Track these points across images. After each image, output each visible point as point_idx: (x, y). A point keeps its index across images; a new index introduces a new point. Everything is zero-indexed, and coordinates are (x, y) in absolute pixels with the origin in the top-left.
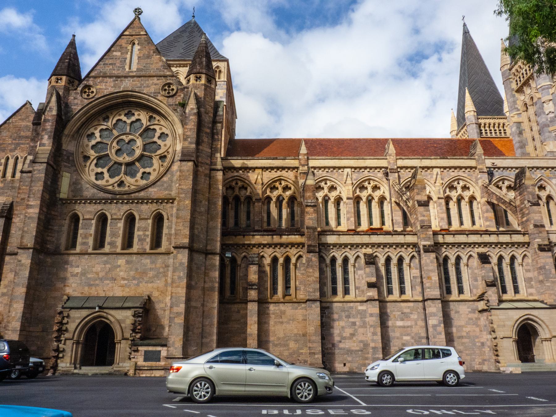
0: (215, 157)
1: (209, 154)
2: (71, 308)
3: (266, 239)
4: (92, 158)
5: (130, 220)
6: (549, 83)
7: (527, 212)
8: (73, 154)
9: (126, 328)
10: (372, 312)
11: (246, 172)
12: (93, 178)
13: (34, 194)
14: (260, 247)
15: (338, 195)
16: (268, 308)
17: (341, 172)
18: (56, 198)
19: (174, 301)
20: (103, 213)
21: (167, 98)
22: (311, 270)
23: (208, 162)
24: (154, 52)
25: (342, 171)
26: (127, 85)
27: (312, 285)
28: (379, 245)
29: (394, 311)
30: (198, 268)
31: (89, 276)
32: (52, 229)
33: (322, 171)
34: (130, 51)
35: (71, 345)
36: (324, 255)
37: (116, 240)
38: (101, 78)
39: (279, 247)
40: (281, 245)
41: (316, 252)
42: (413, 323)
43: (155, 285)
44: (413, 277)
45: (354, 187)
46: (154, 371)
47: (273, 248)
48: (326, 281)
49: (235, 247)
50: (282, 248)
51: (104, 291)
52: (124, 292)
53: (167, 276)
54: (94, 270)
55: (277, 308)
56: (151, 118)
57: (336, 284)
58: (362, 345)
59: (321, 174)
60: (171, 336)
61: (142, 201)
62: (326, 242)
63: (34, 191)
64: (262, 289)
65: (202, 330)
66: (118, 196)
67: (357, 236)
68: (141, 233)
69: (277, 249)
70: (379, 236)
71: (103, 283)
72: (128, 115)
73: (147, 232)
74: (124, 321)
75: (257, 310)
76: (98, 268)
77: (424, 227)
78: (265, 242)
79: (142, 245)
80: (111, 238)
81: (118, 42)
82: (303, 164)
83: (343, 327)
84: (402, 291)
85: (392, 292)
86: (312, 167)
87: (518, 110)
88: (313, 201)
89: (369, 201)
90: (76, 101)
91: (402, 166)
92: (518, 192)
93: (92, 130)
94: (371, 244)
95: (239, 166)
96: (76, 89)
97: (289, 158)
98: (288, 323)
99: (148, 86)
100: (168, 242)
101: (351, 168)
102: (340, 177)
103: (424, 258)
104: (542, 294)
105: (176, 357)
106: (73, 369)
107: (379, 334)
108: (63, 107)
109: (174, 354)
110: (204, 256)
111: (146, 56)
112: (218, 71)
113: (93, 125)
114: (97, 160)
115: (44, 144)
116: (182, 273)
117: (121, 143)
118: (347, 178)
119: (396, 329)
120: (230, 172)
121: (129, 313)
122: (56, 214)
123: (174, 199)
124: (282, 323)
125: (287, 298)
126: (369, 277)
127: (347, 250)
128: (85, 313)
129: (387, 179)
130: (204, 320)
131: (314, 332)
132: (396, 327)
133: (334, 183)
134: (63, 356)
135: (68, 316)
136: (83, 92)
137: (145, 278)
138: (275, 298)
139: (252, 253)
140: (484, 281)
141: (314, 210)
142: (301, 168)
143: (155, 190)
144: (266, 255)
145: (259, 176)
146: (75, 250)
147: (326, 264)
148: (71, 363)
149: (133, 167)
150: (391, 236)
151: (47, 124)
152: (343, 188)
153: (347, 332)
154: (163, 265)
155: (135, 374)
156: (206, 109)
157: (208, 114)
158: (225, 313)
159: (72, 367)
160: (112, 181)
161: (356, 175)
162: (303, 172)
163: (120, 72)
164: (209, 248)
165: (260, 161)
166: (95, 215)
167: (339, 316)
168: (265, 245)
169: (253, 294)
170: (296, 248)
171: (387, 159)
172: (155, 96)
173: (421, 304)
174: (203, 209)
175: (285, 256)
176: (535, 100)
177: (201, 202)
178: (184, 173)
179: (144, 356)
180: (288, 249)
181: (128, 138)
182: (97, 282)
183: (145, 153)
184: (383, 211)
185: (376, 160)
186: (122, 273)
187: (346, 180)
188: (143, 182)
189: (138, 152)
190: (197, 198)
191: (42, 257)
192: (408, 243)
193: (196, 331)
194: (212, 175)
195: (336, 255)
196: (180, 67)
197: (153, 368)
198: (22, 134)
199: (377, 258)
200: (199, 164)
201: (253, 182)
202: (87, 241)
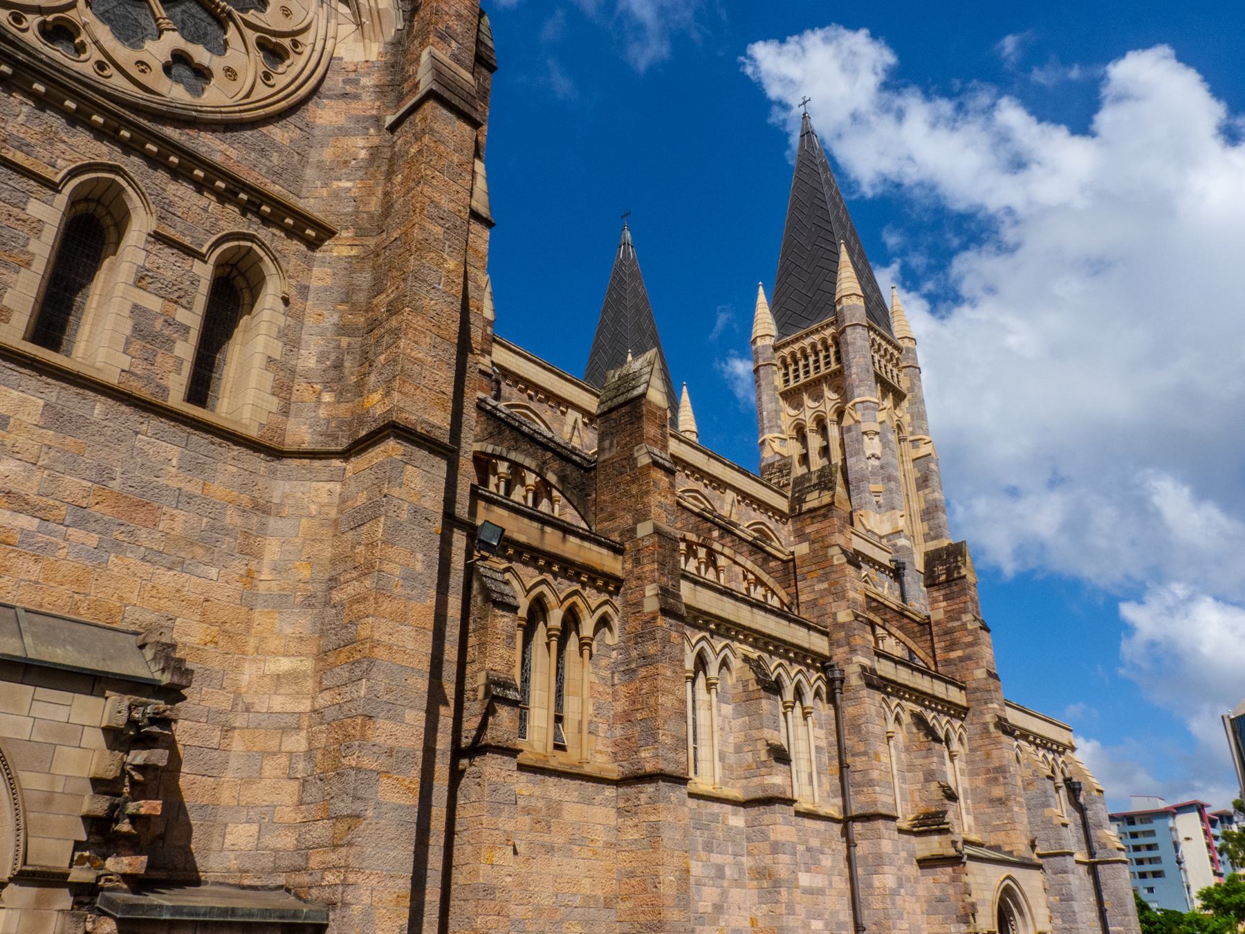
6: (876, 401)
7: (970, 639)
9: (49, 800)
19: (381, 688)
22: (669, 674)
43: (192, 585)
53: (258, 556)
55: (537, 791)
60: (360, 878)
73: (181, 311)
77: (860, 619)
78: (522, 538)
87: (782, 432)
92: (943, 592)
100: (275, 400)
103: (867, 700)
104: (996, 829)
123: (325, 233)
124: (550, 849)
137: (143, 534)
140: (934, 786)
150: (786, 623)
154: (245, 499)
173: (837, 828)
176: (847, 422)
178: (442, 148)
188: (175, 93)
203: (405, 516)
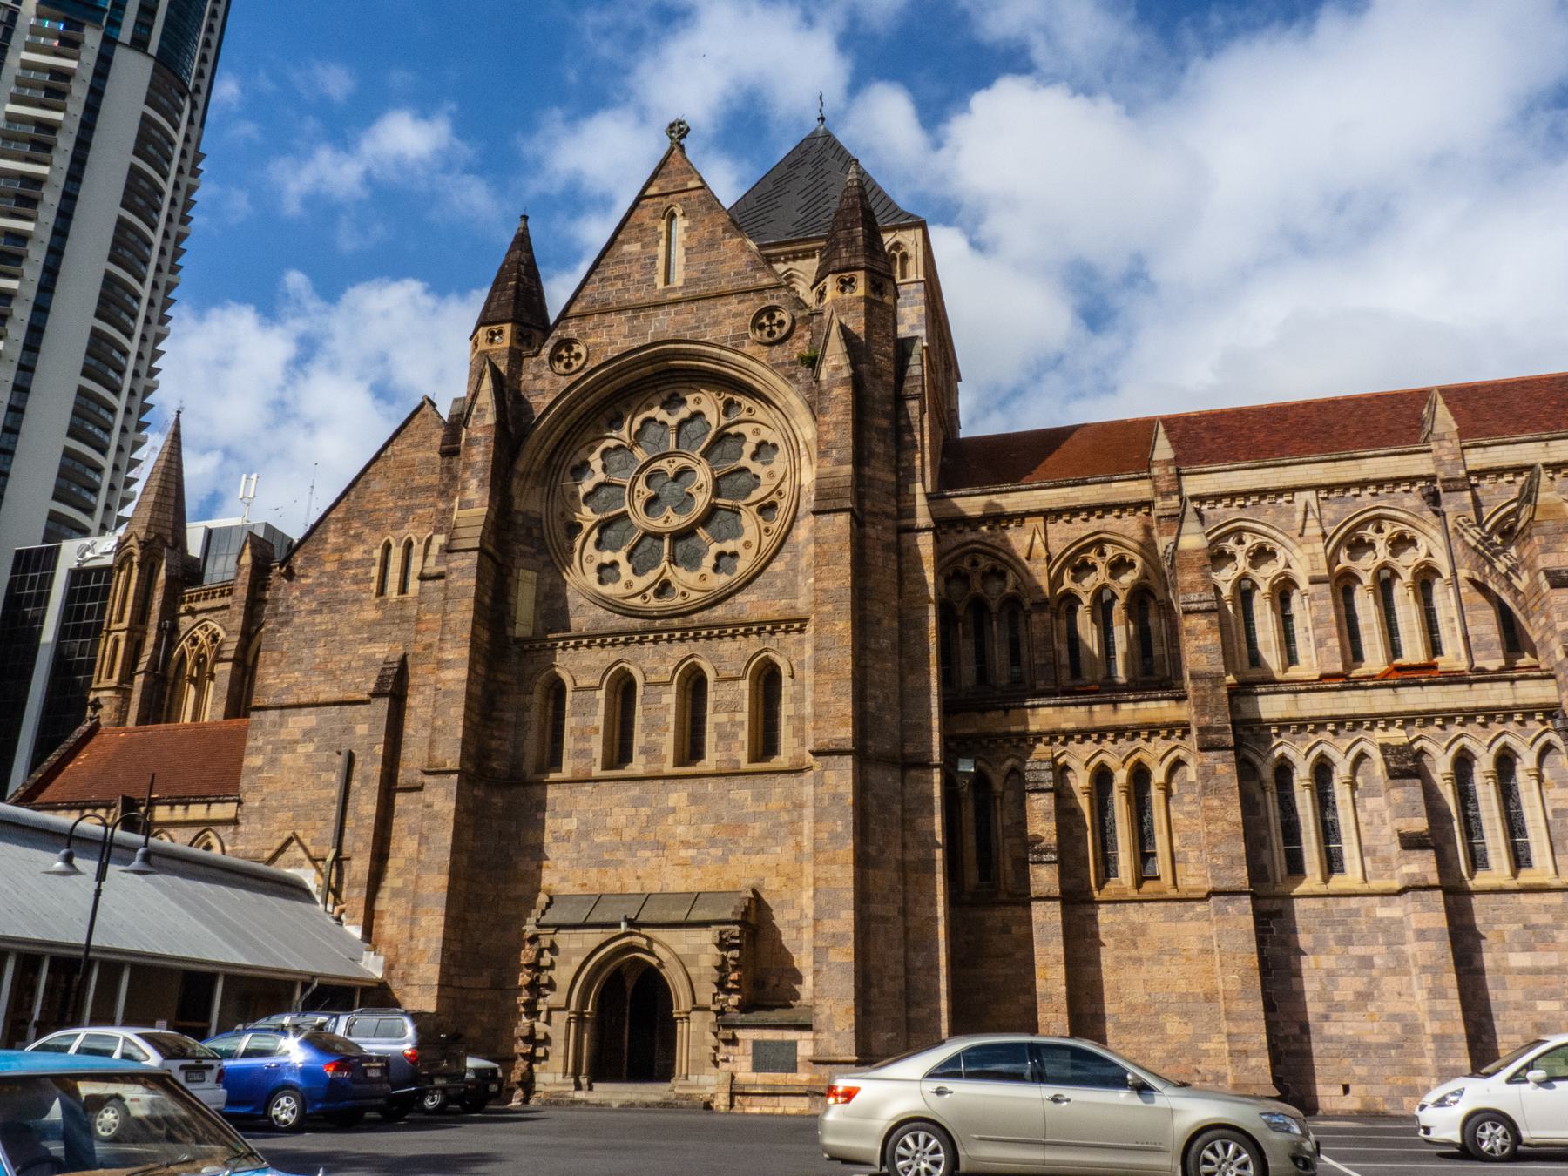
0: (908, 494)
1: (893, 488)
2: (559, 927)
3: (1072, 717)
4: (587, 526)
5: (694, 686)
8: (540, 521)
9: (700, 977)
10: (1424, 926)
12: (592, 577)
13: (453, 632)
14: (1056, 739)
16: (1094, 917)
17: (1285, 505)
18: (507, 638)
19: (823, 902)
21: (767, 349)
22: (1216, 803)
23: (892, 509)
24: (725, 231)
25: (1289, 502)
26: (662, 325)
27: (1223, 848)
28: (1428, 717)
29: (1499, 921)
31: (599, 839)
32: (501, 720)
33: (1226, 506)
34: (664, 235)
35: (563, 1025)
36: (1252, 756)
37: (661, 739)
38: (596, 317)
39: (1111, 736)
40: (1119, 731)
41: (1227, 748)
43: (769, 859)
44: (1555, 811)
46: (781, 1098)
47: (1095, 742)
48: (1264, 833)
49: (985, 742)
50: (1121, 741)
51: (638, 878)
53: (800, 833)
54: (610, 821)
55: (1119, 918)
56: (729, 405)
57: (1299, 842)
58: (1398, 1029)
60: (823, 1002)
61: (721, 630)
62: (1255, 716)
63: (452, 624)
65: (907, 982)
66: (658, 623)
68: (723, 718)
69: (1106, 744)
70: (1426, 689)
71: (635, 856)
74: (694, 959)
76: (619, 817)
78: (1070, 726)
79: (728, 749)
80: (648, 735)
81: (632, 218)
82: (1165, 489)
83: (1331, 974)
84: (1519, 858)
85: (1485, 860)
86: (1193, 498)
88: (1205, 597)
89: (1384, 586)
90: (539, 384)
91: (1485, 466)
93: (582, 454)
94: (1401, 714)
95: (978, 513)
96: (537, 354)
97: (1121, 477)
98: (1158, 962)
99: (716, 323)
100: (796, 740)
101: (1317, 488)
102: (1283, 520)
105: (840, 1059)
106: (573, 1088)
107: (1454, 993)
108: (509, 403)
109: (833, 1050)
110: (897, 773)
112: (898, 255)
114: (601, 532)
115: (469, 501)
116: (839, 823)
117: (659, 481)
119: (1509, 979)
120: (952, 532)
121: (707, 937)
122: (509, 678)
123: (804, 621)
124: (1138, 961)
125: (1148, 887)
126: (1403, 816)
127: (1325, 735)
128: (593, 938)
129: (1436, 513)
130: (912, 954)
131: (1239, 987)
132: (1509, 971)
133: (1266, 539)
135: (553, 949)
136: (555, 357)
137: (741, 841)
138: (1111, 887)
141: (1212, 623)
142: (1159, 503)
143: (753, 597)
144: (1073, 763)
145: (1037, 535)
146: (560, 771)
148: (565, 1073)
149: (692, 542)
150: (1465, 687)
151: (474, 451)
152: (1298, 553)
153: (1347, 989)
154: (789, 804)
155: (732, 1106)
156: (875, 365)
159: (568, 1084)
160: (640, 583)
161: (1335, 507)
162: (1167, 513)
163: (643, 296)
164: (909, 749)
165: (1036, 493)
166: (603, 678)
167: (1316, 939)
168: (1069, 735)
169: (1044, 878)
170: (1165, 738)
171: (1430, 451)
172: (736, 345)
174: (885, 643)
175: (1130, 762)
177: (879, 622)
178: (825, 547)
179: (754, 1054)
180: (1139, 742)
181: (674, 465)
182: (619, 855)
183: (719, 501)
184: (1433, 610)
185: (1396, 458)
186: (680, 830)
187: (1303, 527)
188: (720, 581)
189: (701, 501)
192: (1526, 706)
194: (905, 545)
195: (1291, 754)
196: (795, 259)
197: (777, 1091)
198: (419, 481)
200: (867, 518)
201: (1022, 554)
202: (586, 746)
203: (827, 802)
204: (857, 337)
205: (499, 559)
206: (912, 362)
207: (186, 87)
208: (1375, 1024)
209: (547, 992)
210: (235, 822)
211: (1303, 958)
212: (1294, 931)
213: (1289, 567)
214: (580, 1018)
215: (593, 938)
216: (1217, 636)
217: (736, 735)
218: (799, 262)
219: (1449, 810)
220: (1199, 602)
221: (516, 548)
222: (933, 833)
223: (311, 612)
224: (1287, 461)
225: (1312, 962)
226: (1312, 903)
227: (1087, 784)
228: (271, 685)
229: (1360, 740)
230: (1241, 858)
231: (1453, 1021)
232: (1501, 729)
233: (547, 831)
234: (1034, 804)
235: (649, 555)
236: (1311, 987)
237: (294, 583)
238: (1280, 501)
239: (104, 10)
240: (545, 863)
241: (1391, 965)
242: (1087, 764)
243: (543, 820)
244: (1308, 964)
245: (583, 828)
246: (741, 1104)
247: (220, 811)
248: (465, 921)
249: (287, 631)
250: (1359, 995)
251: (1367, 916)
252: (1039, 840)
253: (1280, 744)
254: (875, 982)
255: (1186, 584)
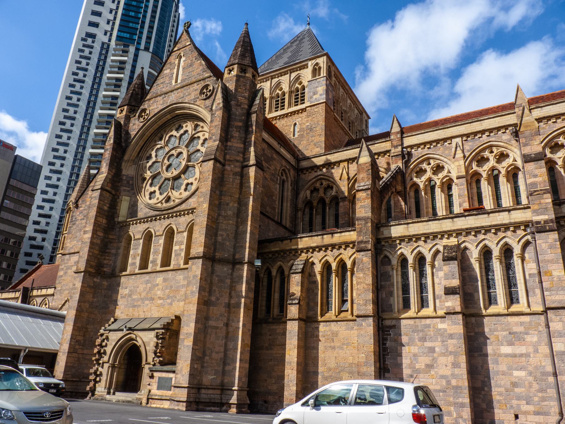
0: (248, 152)
1: (242, 150)
2: (110, 331)
3: (315, 241)
4: (148, 178)
5: (170, 234)
8: (133, 178)
10: (452, 332)
11: (330, 168)
14: (309, 252)
15: (446, 176)
16: (318, 328)
17: (448, 145)
18: (115, 222)
20: (149, 231)
21: (204, 101)
22: (361, 275)
23: (241, 159)
24: (196, 59)
25: (449, 144)
26: (172, 98)
27: (363, 295)
28: (468, 232)
29: (496, 330)
30: (221, 281)
31: (134, 297)
32: (110, 253)
34: (177, 65)
36: (388, 254)
38: (153, 99)
39: (330, 248)
40: (333, 246)
41: (368, 250)
42: (531, 349)
44: (530, 275)
45: (468, 161)
47: (324, 251)
48: (392, 289)
49: (282, 254)
50: (335, 250)
51: (144, 312)
52: (159, 313)
55: (328, 328)
56: (196, 126)
57: (409, 294)
58: (444, 383)
59: (421, 153)
61: (180, 214)
62: (389, 236)
64: (312, 304)
67: (434, 222)
69: (329, 252)
70: (467, 218)
71: (144, 303)
72: (177, 130)
74: (149, 343)
75: (297, 331)
79: (178, 260)
83: (415, 355)
84: (512, 299)
85: (496, 300)
86: (407, 147)
88: (367, 183)
89: (494, 179)
91: (541, 116)
93: (149, 152)
94: (454, 231)
95: (322, 163)
96: (135, 116)
97: (379, 141)
98: (342, 348)
101: (461, 136)
102: (447, 152)
105: (182, 386)
106: (106, 394)
107: (464, 365)
108: (123, 135)
109: (181, 382)
110: (231, 266)
111: (189, 65)
112: (317, 68)
113: (151, 146)
114: (152, 180)
116: (194, 287)
117: (171, 159)
118: (456, 151)
119: (500, 359)
120: (313, 172)
121: (152, 334)
122: (114, 237)
124: (334, 348)
125: (343, 315)
126: (448, 279)
127: (421, 243)
128: (120, 334)
129: (517, 140)
130: (229, 343)
132: (500, 355)
133: (440, 161)
134: (100, 380)
135: (107, 338)
136: (140, 116)
138: (328, 316)
139: (298, 260)
141: (368, 195)
142: (392, 151)
144: (316, 261)
145: (344, 170)
146: (126, 271)
147: (392, 266)
150: (486, 215)
152: (453, 166)
153: (421, 364)
155: (147, 403)
156: (238, 101)
157: (240, 106)
158: (270, 335)
159: (104, 392)
161: (470, 144)
162: (395, 154)
164: (237, 256)
165: (345, 152)
167: (410, 339)
168: (314, 249)
169: (293, 311)
170: (352, 248)
171: (515, 113)
172: (195, 102)
173: (542, 318)
175: (338, 259)
177: (228, 204)
179: (158, 383)
180: (342, 251)
181: (177, 152)
182: (139, 303)
183: (189, 163)
184: (518, 186)
185: (499, 118)
186: (159, 292)
187: (455, 154)
188: (186, 194)
190: (222, 201)
191: (98, 280)
192: (515, 223)
193: (214, 355)
196: (281, 76)
199: (467, 252)
200: (227, 162)
203: (191, 278)
204: (232, 91)
205: (113, 192)
206: (257, 98)
207: (162, 61)
208: (434, 380)
209: (104, 356)
210: (53, 295)
211: (403, 348)
212: (400, 335)
213: (450, 173)
214: (113, 366)
215: (120, 334)
216: (370, 200)
217: (180, 254)
218: (283, 77)
219: (477, 276)
220: (364, 186)
221: (122, 188)
222: (241, 291)
223: (81, 220)
224: (449, 126)
225: (407, 349)
226: (411, 322)
227: (320, 270)
228: (68, 246)
229: (436, 244)
230: (370, 300)
231: (462, 379)
232: (503, 235)
233: (119, 294)
234: (293, 279)
235: (166, 187)
236: (406, 361)
237: (78, 210)
238: (446, 144)
239: (135, 40)
240: (117, 307)
241: (443, 351)
242: (320, 261)
243: (119, 290)
244: (405, 351)
245: (130, 293)
246: (151, 403)
247: (50, 291)
248: (87, 328)
249: (74, 227)
250: (427, 366)
251: (434, 327)
252: (293, 294)
253: (401, 248)
254: (208, 354)
255: (360, 178)
